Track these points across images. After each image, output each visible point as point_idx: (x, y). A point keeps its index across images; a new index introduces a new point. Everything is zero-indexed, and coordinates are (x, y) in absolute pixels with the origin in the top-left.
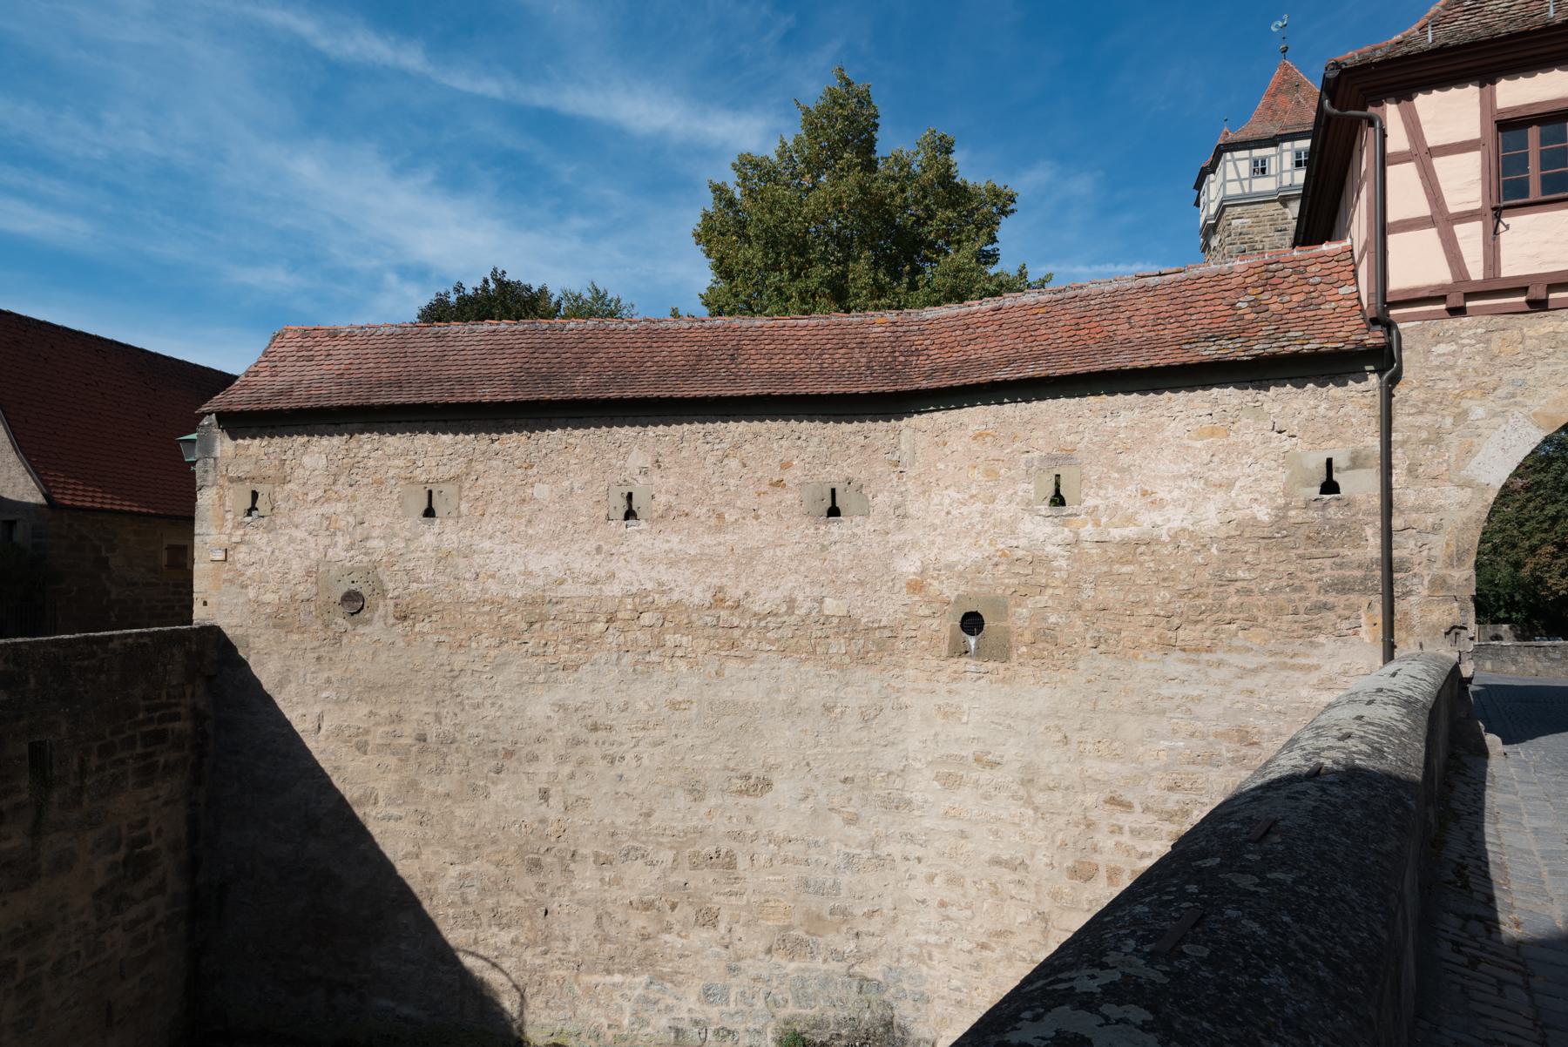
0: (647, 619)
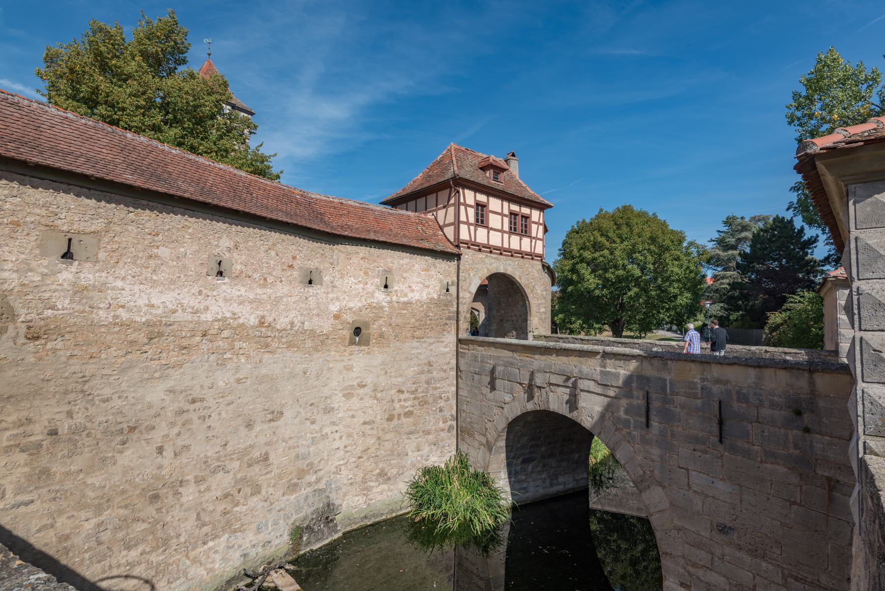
0: (226, 333)
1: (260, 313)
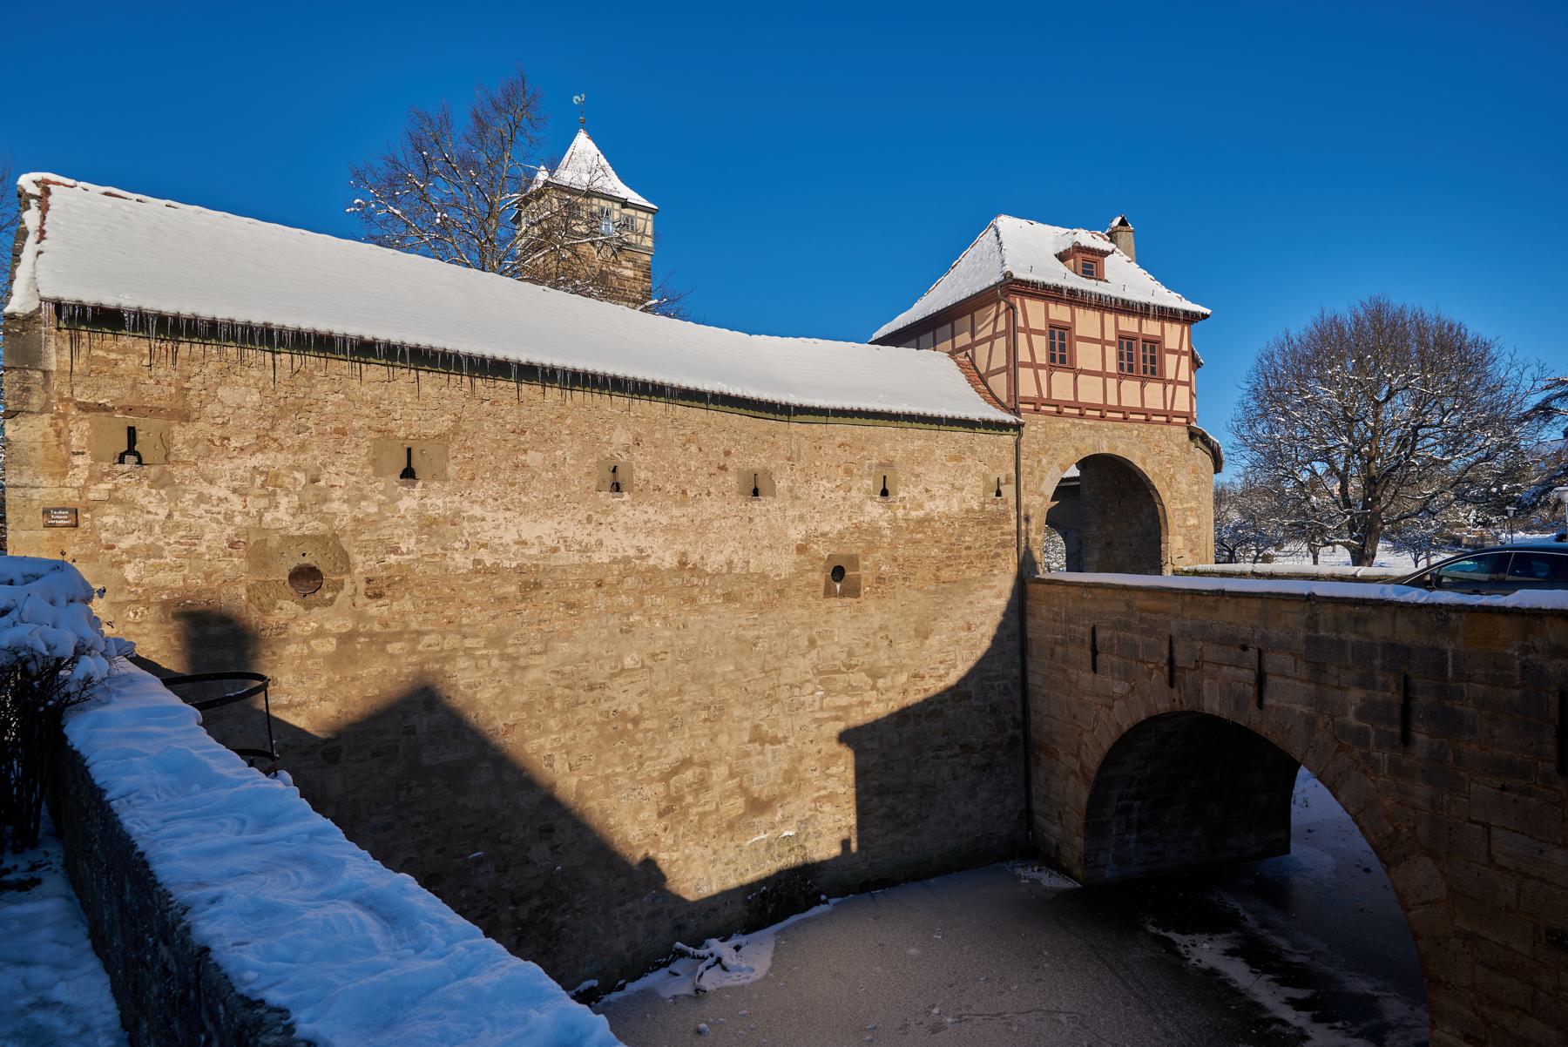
0: (630, 582)
1: (679, 547)
